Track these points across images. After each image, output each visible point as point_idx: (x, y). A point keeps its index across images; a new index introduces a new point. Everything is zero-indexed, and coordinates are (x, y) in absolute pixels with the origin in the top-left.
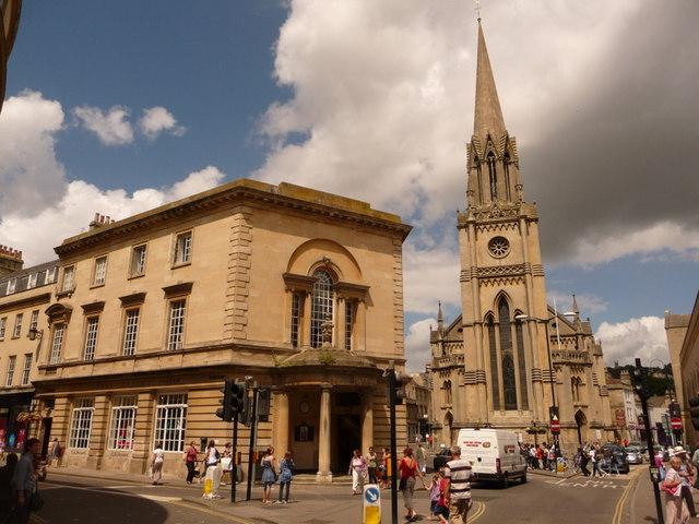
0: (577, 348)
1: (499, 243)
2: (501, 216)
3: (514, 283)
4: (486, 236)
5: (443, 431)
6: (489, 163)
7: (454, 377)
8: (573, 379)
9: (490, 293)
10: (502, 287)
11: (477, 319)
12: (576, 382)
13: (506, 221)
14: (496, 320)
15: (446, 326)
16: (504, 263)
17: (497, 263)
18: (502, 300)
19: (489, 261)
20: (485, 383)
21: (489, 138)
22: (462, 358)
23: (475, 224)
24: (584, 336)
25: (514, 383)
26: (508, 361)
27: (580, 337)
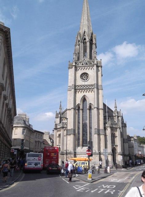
1: (85, 76)
2: (87, 64)
3: (90, 92)
6: (84, 43)
9: (80, 95)
10: (85, 94)
13: (88, 66)
14: (81, 107)
16: (86, 83)
17: (83, 83)
18: (84, 99)
19: (80, 82)
22: (66, 124)
23: (76, 67)
25: (87, 135)
26: (84, 125)
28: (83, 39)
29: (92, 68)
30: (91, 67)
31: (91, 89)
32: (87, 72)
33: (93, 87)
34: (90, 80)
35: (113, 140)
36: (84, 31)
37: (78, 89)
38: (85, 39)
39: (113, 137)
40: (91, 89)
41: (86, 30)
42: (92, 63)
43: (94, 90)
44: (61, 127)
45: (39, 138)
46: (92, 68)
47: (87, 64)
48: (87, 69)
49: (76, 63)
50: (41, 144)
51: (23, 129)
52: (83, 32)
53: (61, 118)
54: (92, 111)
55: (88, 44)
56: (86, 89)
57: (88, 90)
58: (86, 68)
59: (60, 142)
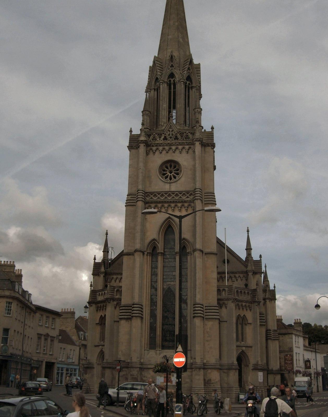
0: (246, 285)
1: (170, 169)
2: (176, 138)
4: (158, 159)
5: (95, 370)
7: (110, 312)
8: (238, 317)
11: (138, 246)
12: (242, 321)
13: (180, 144)
15: (112, 255)
16: (174, 187)
17: (167, 187)
19: (159, 185)
20: (142, 318)
21: (172, 57)
22: (119, 291)
23: (147, 145)
24: (255, 273)
27: (250, 274)
28: (168, 74)
29: (190, 148)
30: (187, 147)
31: (185, 202)
32: (176, 159)
33: (192, 197)
34: (183, 179)
35: (240, 332)
36: (169, 54)
37: (152, 203)
38: (172, 75)
39: (240, 326)
40: (185, 202)
41: (175, 54)
42: (190, 136)
43: (192, 204)
44: (107, 299)
45: (48, 327)
46: (190, 148)
47: (176, 138)
48: (177, 151)
49: (149, 136)
50: (52, 341)
51: (7, 302)
52: (168, 58)
53: (106, 274)
54: (189, 257)
55: (180, 88)
56: (173, 202)
57: (179, 205)
58: (174, 148)
59: (102, 338)
